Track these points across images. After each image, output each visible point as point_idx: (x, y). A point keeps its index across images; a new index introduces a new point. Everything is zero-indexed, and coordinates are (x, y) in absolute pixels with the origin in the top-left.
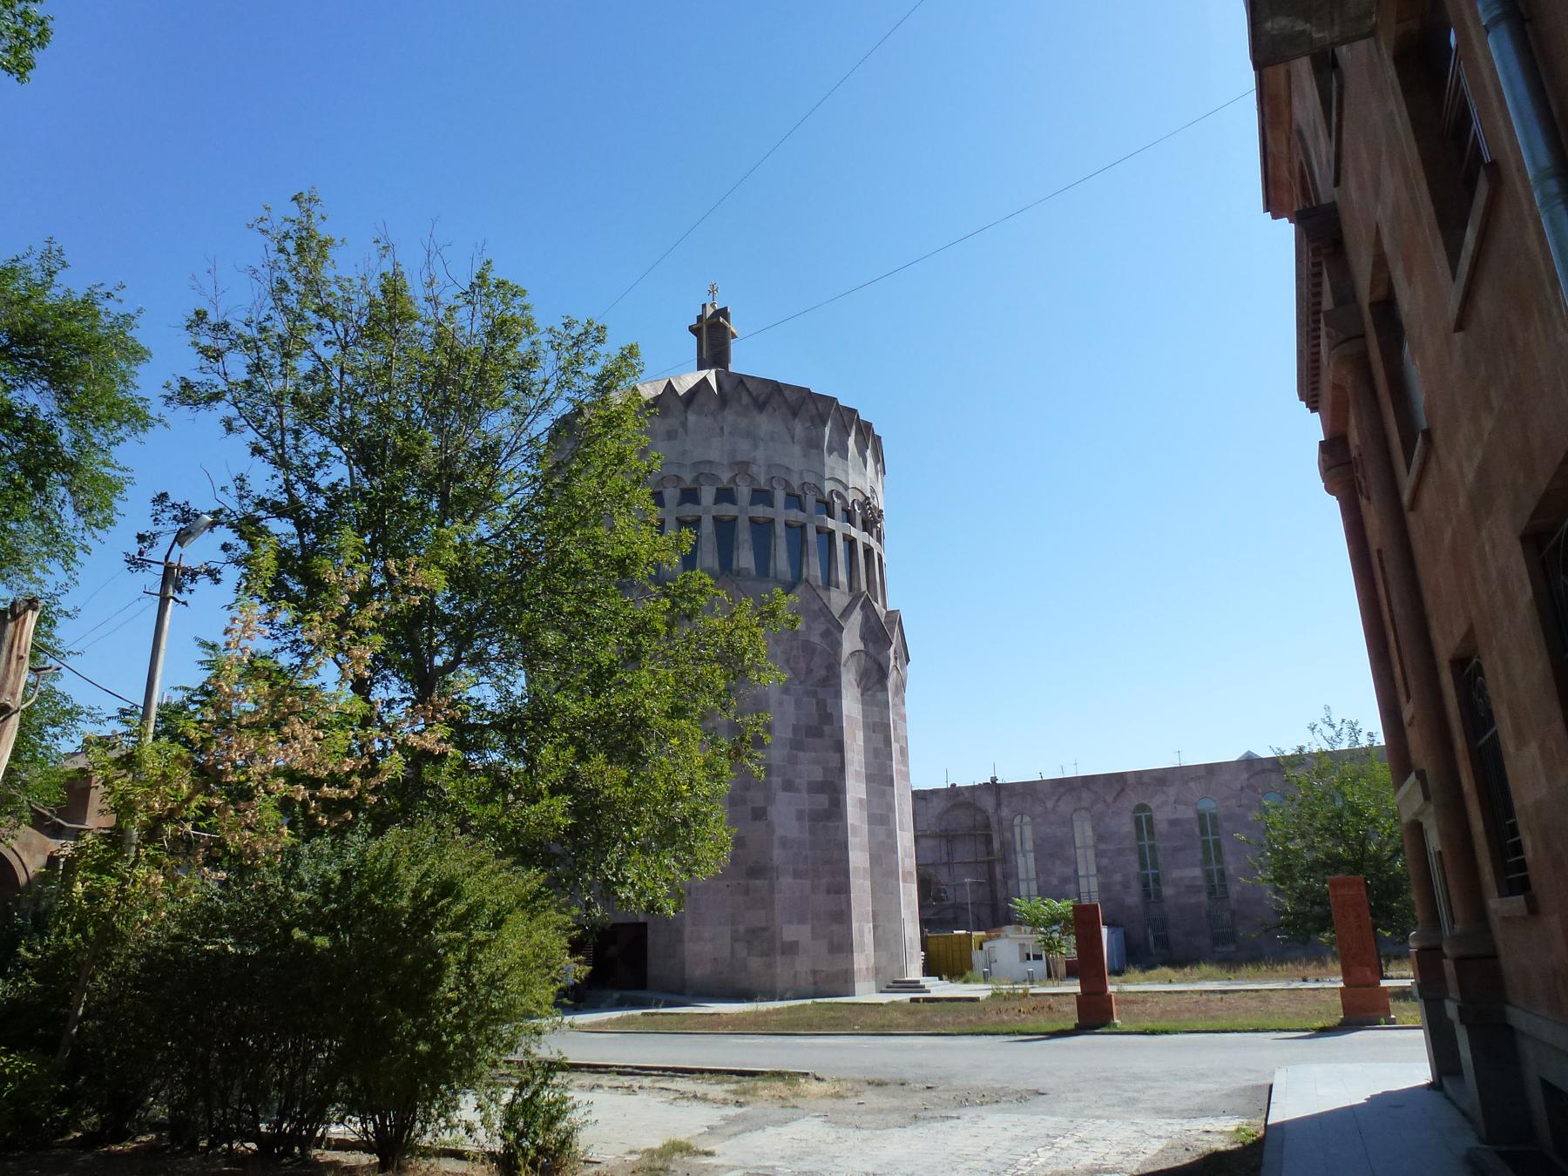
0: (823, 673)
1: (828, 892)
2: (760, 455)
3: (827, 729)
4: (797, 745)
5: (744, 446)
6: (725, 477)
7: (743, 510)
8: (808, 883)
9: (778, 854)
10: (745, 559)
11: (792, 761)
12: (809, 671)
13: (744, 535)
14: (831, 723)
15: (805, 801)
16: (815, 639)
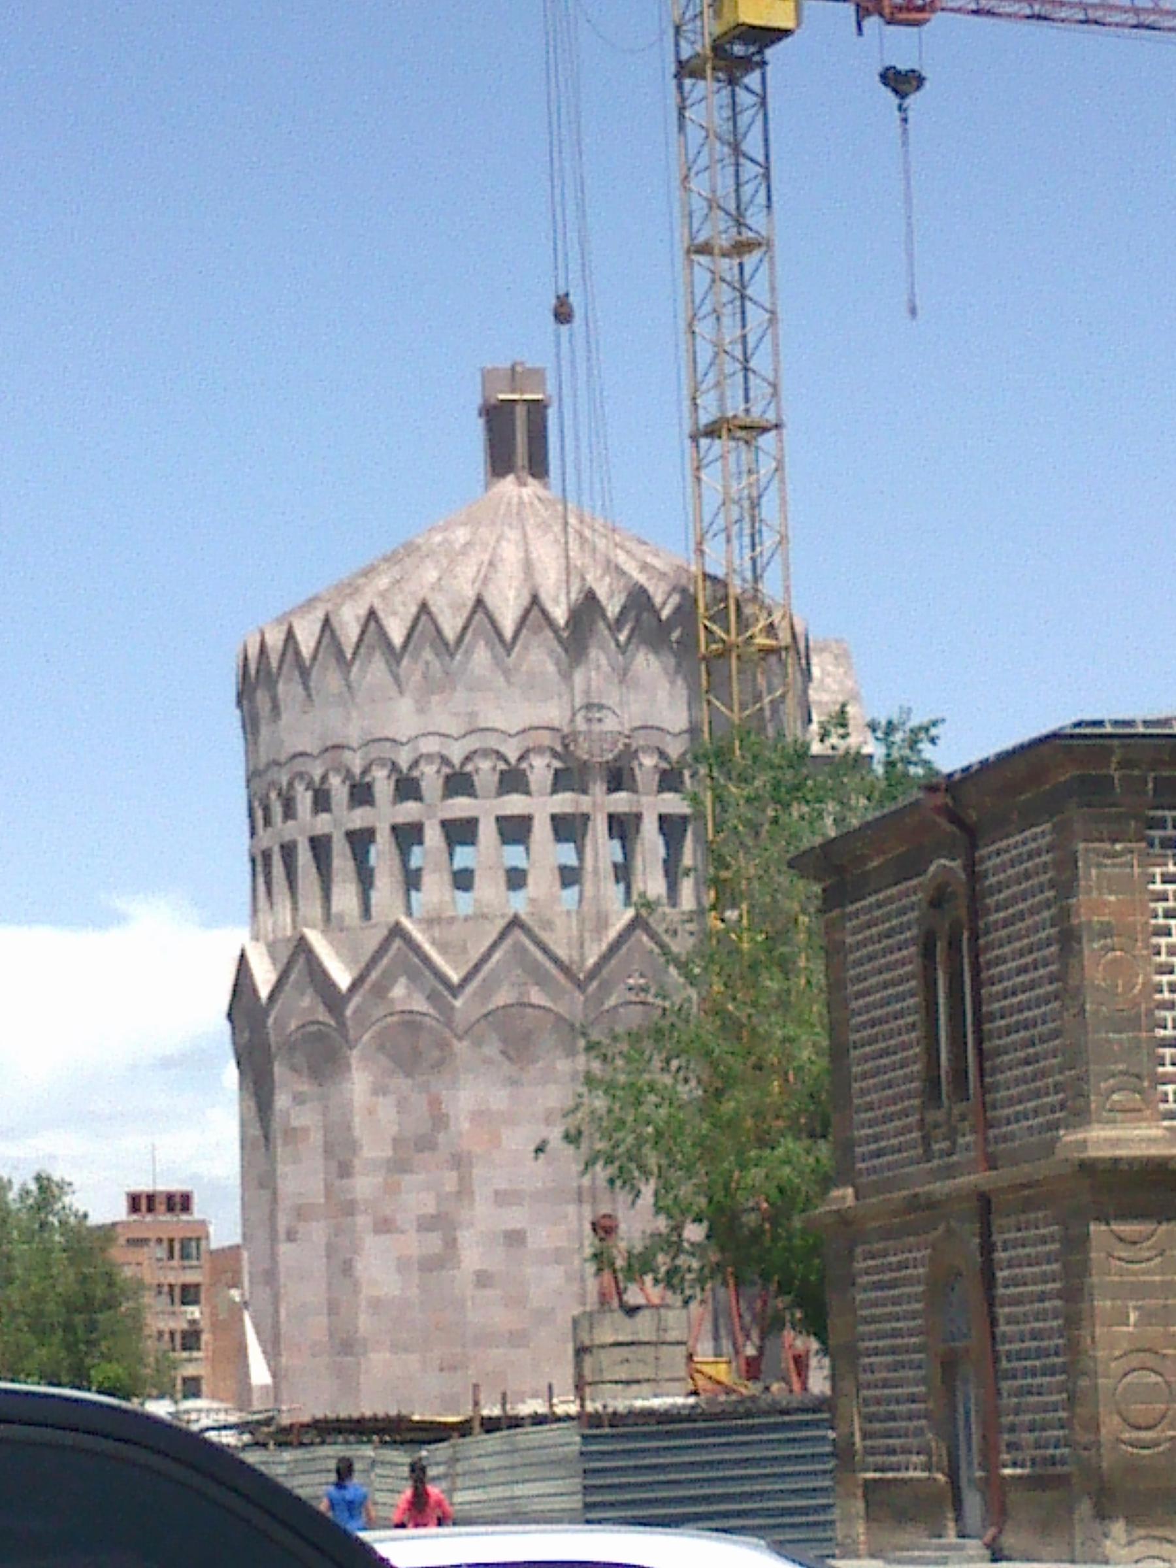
0: (436, 1054)
1: (442, 1370)
2: (353, 735)
3: (441, 1137)
4: (399, 1166)
6: (317, 774)
8: (414, 1357)
9: (365, 1323)
10: (345, 898)
11: (391, 1189)
12: (417, 1054)
13: (342, 861)
14: (447, 1127)
15: (413, 1244)
16: (420, 1004)
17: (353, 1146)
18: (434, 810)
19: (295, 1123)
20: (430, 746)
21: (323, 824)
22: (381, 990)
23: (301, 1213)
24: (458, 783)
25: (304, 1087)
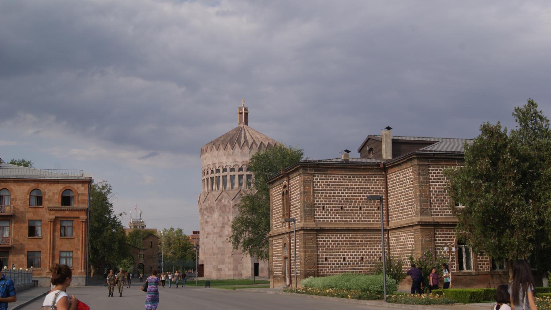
2: (217, 162)
5: (215, 159)
7: (215, 175)
11: (221, 231)
12: (226, 210)
16: (226, 203)
17: (216, 224)
18: (228, 174)
19: (208, 220)
20: (228, 164)
21: (212, 175)
22: (220, 200)
23: (208, 234)
24: (232, 170)
25: (209, 215)
